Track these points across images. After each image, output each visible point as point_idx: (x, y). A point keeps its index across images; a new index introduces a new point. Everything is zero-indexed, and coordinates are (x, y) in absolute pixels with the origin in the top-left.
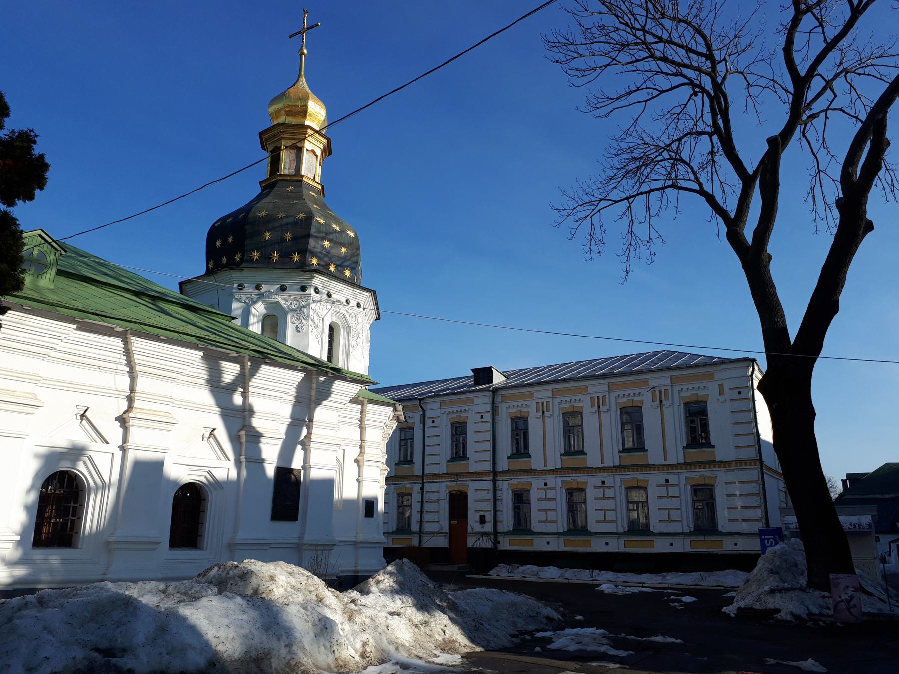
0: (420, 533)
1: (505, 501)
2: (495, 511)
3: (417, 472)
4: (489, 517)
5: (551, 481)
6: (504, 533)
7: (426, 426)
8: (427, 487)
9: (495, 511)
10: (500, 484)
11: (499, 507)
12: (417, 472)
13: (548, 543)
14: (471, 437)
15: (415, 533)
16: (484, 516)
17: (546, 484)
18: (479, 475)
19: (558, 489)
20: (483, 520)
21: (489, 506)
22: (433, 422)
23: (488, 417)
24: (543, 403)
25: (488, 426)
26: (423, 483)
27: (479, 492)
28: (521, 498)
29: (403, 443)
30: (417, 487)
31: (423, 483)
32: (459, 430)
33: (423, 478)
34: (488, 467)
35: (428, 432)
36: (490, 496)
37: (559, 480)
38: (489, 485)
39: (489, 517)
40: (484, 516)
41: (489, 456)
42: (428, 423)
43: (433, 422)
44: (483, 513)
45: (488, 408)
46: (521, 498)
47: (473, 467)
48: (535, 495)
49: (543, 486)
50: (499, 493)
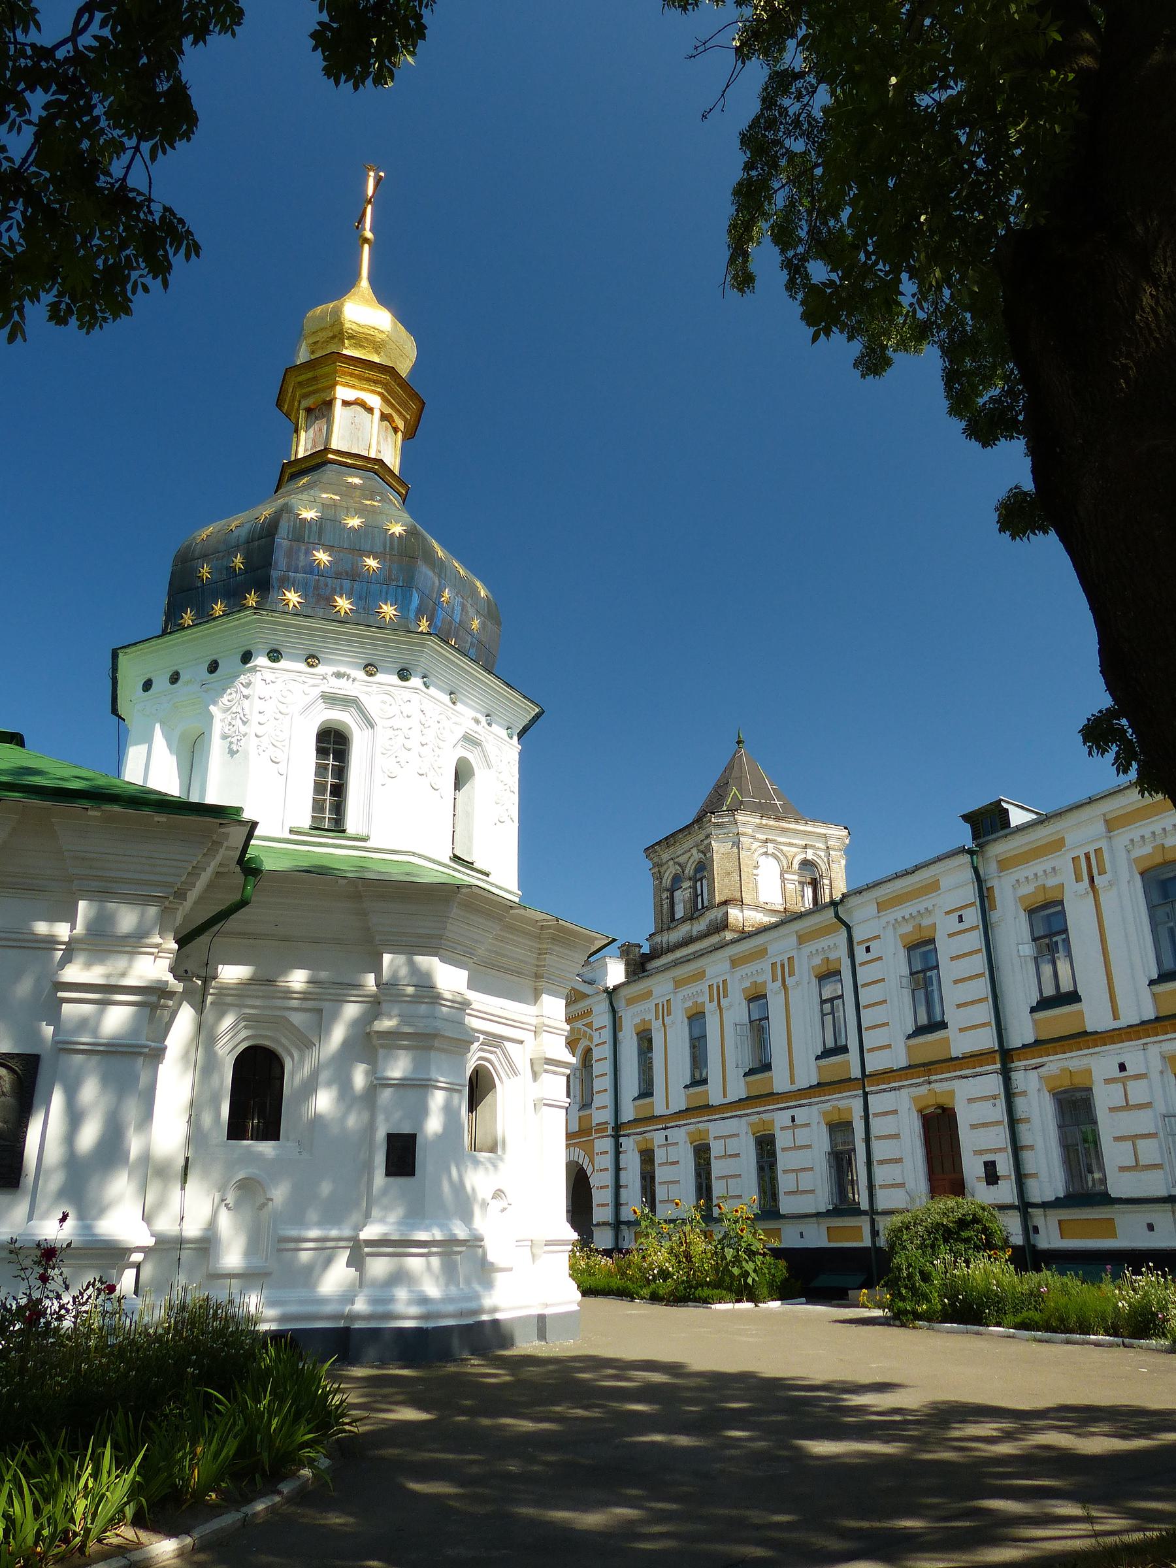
0: (873, 1212)
1: (1036, 1121)
2: (1017, 1148)
3: (856, 1073)
4: (1004, 1166)
5: (1133, 1054)
6: (1045, 1205)
7: (858, 961)
8: (877, 1103)
9: (1017, 1148)
10: (1020, 1079)
11: (1025, 1138)
12: (856, 1073)
13: (1151, 1227)
14: (948, 970)
15: (864, 1213)
16: (993, 1163)
17: (1122, 1067)
18: (975, 1058)
19: (1155, 1076)
20: (991, 1175)
21: (999, 1137)
22: (868, 950)
23: (973, 917)
24: (1087, 856)
25: (975, 940)
26: (866, 1094)
27: (975, 1105)
28: (1075, 1107)
29: (827, 1007)
30: (857, 1105)
31: (866, 1094)
32: (922, 953)
33: (865, 1081)
34: (986, 1040)
35: (864, 975)
36: (998, 1112)
37: (1154, 1051)
38: (992, 1083)
39: (1004, 1166)
40: (993, 1163)
41: (984, 1013)
42: (860, 951)
43: (868, 950)
44: (989, 1157)
45: (969, 893)
46: (1075, 1107)
47: (960, 1043)
48: (1104, 1098)
49: (1116, 1073)
50: (1020, 1102)
